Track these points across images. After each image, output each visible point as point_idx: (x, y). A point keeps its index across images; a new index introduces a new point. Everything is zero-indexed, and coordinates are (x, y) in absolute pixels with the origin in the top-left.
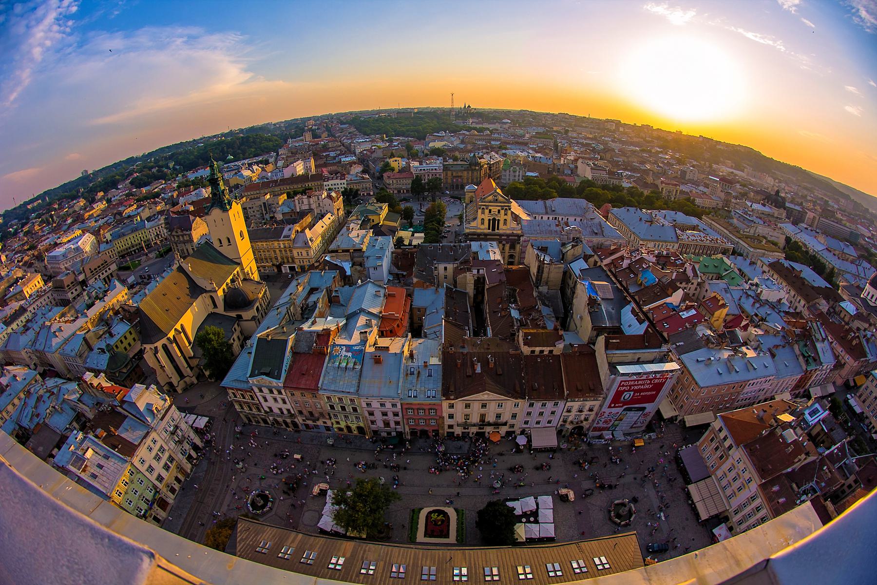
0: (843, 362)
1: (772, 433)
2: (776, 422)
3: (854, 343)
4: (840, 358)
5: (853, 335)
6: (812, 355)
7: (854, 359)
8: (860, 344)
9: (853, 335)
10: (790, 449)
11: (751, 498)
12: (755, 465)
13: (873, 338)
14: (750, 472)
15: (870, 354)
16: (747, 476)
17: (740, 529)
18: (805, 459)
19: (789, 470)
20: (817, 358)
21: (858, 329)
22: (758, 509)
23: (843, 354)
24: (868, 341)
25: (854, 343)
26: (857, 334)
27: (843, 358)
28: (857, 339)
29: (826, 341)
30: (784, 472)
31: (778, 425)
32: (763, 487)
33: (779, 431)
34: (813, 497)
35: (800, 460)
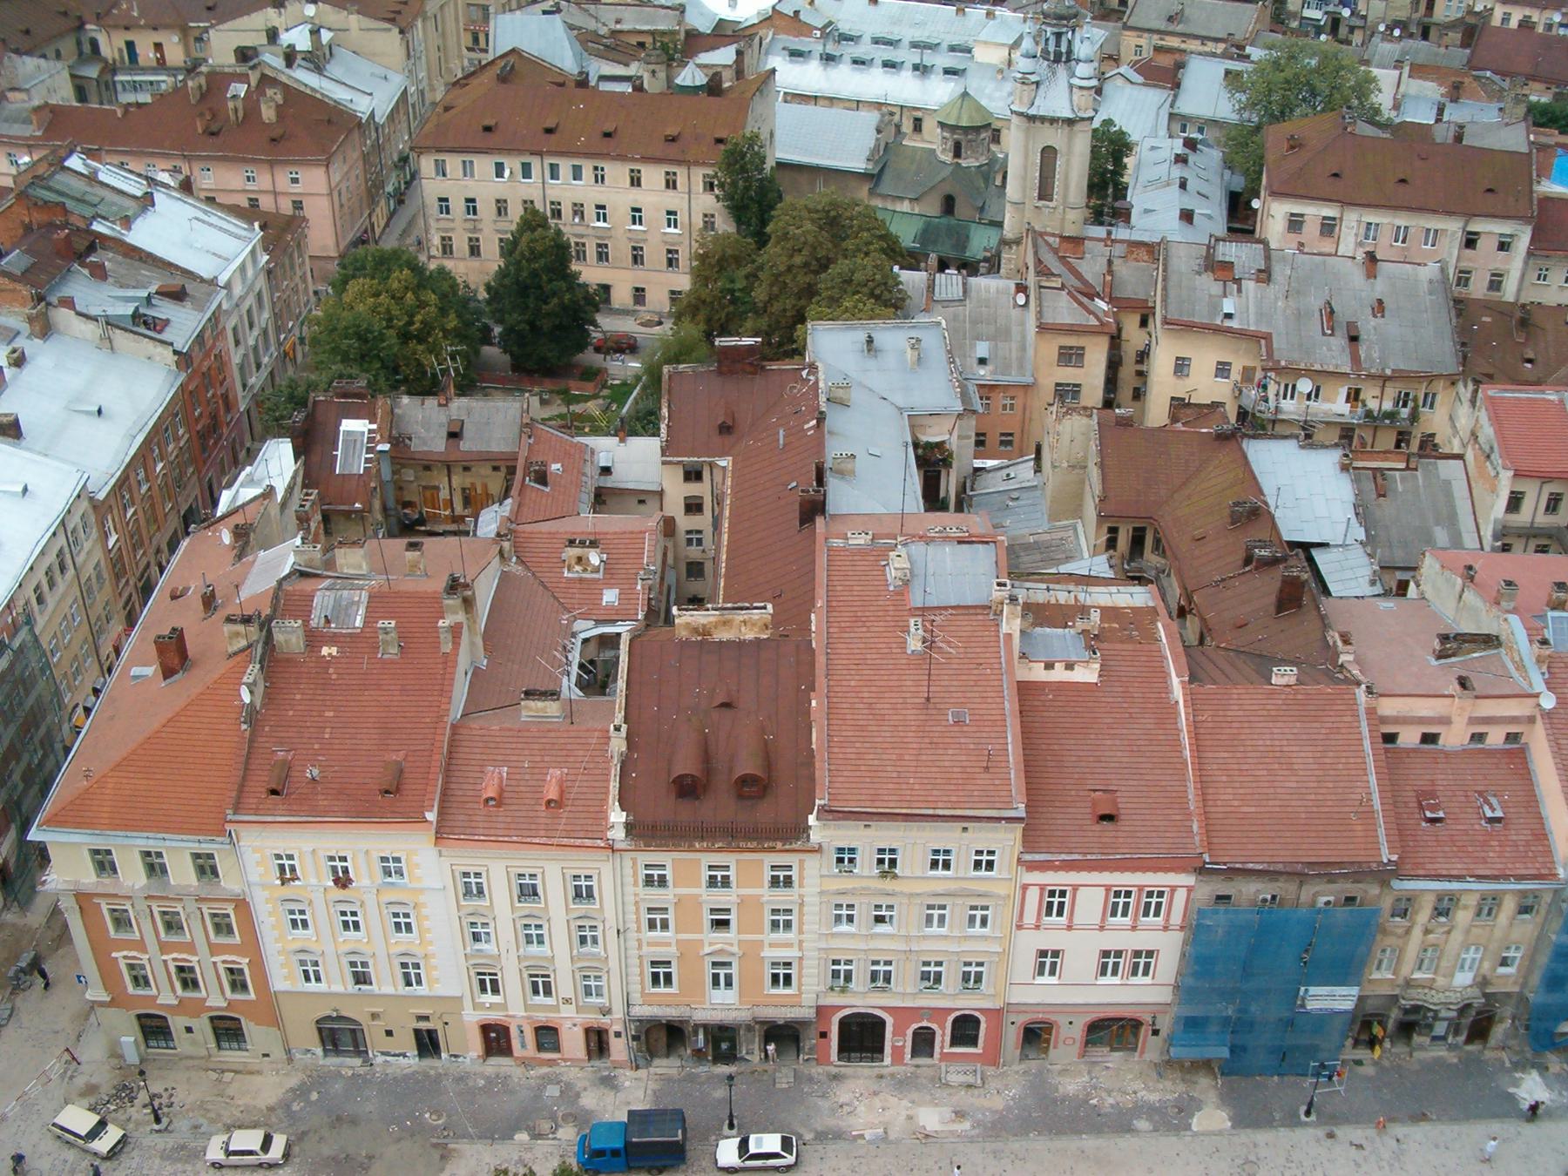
0: (286, 207)
3: (268, 113)
4: (266, 203)
5: (241, 89)
6: (153, 289)
7: (316, 163)
8: (296, 99)
9: (241, 89)
13: (326, 36)
15: (357, 97)
20: (177, 281)
21: (244, 54)
23: (263, 180)
24: (317, 59)
25: (268, 113)
26: (254, 78)
27: (275, 193)
28: (270, 92)
29: (159, 197)
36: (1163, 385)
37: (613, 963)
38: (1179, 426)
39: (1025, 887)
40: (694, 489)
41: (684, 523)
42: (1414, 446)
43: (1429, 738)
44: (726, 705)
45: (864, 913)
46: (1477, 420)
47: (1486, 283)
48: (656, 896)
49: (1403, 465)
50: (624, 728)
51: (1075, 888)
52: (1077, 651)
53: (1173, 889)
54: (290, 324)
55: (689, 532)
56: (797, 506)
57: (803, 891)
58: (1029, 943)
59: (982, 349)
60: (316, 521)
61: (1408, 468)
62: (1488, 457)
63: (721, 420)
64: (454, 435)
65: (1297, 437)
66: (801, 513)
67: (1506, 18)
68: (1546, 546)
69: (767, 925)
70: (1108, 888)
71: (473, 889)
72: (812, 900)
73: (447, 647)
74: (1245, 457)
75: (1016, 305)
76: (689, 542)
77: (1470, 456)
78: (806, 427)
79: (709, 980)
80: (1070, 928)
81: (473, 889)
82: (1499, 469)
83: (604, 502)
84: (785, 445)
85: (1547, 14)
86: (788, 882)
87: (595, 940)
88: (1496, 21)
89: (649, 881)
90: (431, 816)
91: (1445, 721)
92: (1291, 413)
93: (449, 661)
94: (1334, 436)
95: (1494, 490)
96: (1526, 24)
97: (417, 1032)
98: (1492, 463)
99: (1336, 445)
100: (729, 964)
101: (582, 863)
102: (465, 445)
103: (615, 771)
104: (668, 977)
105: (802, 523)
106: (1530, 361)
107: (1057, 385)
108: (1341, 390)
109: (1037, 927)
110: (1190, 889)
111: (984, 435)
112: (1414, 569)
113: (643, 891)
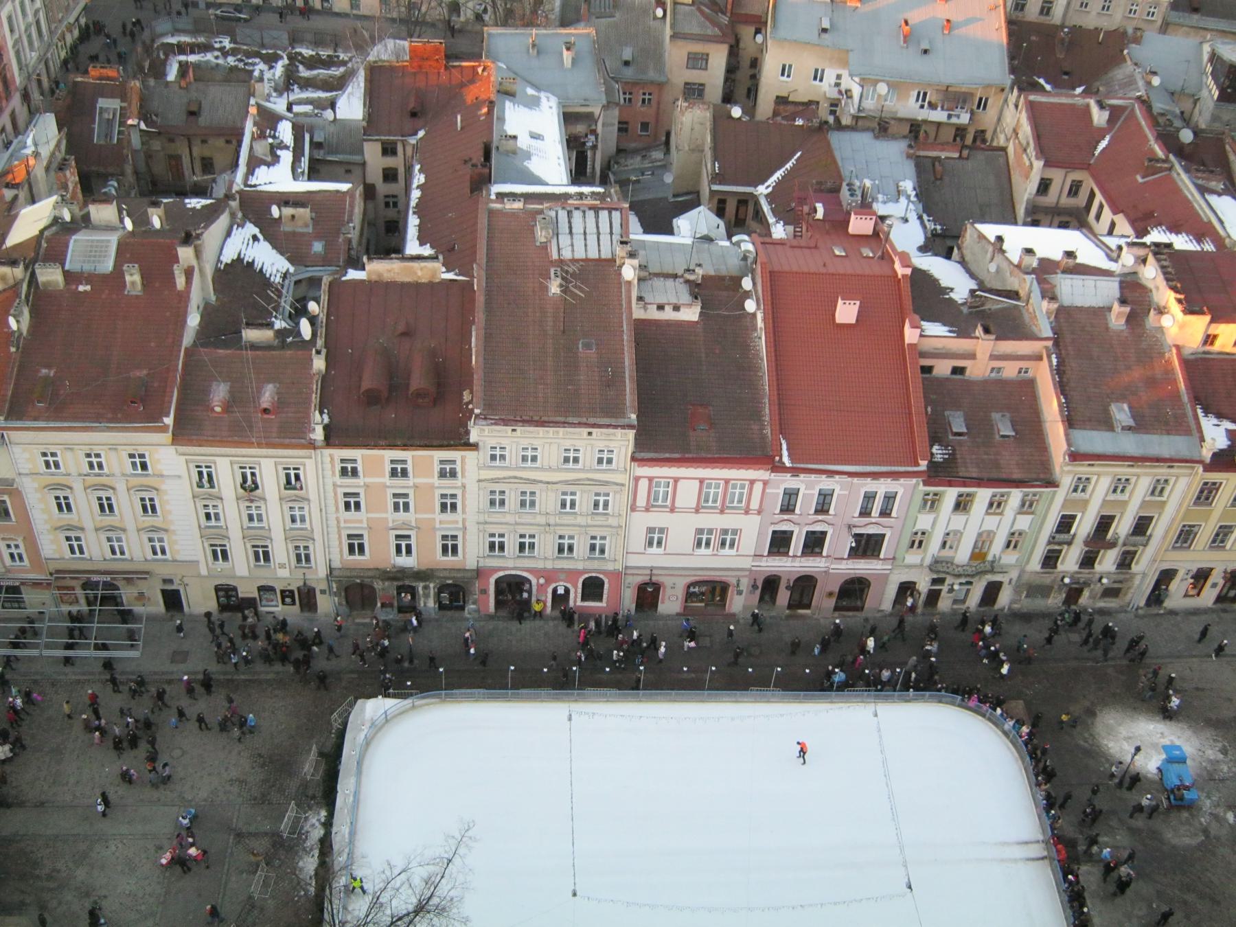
1: (40, 299)
2: (13, 263)
10: (133, 278)
11: (200, 485)
12: (98, 418)
14: (113, 447)
16: (117, 463)
17: (282, 566)
18: (198, 254)
19: (194, 320)
22: (249, 486)
30: (188, 339)
31: (29, 265)
32: (184, 433)
33: (50, 275)
34: (324, 298)
35: (189, 273)
36: (771, 82)
37: (317, 535)
38: (779, 119)
39: (637, 479)
40: (390, 162)
41: (382, 188)
42: (969, 140)
43: (958, 371)
44: (405, 334)
45: (512, 500)
46: (1018, 121)
47: (1038, 9)
48: (350, 484)
49: (956, 155)
50: (324, 351)
51: (676, 480)
52: (685, 297)
53: (752, 482)
54: (60, 15)
55: (386, 196)
56: (468, 177)
57: (464, 481)
58: (641, 522)
59: (627, 54)
60: (72, 177)
61: (960, 157)
62: (1025, 150)
63: (411, 105)
64: (193, 114)
65: (873, 130)
66: (471, 182)
68: (1067, 222)
69: (438, 507)
70: (702, 481)
71: (205, 479)
72: (472, 487)
73: (180, 282)
74: (828, 144)
75: (655, 18)
76: (387, 205)
77: (1011, 150)
78: (479, 113)
79: (393, 550)
80: (672, 510)
81: (205, 479)
82: (1033, 159)
83: (318, 171)
84: (462, 128)
86: (453, 474)
87: (303, 520)
89: (344, 472)
90: (169, 421)
91: (972, 356)
92: (870, 110)
93: (184, 297)
94: (906, 129)
95: (1027, 177)
97: (164, 592)
98: (1027, 155)
99: (905, 137)
100: (409, 537)
101: (292, 457)
102: (203, 121)
103: (315, 387)
104: (361, 547)
105: (472, 191)
106: (1066, 73)
107: (686, 84)
108: (912, 93)
109: (647, 510)
110: (765, 483)
111: (626, 123)
112: (958, 237)
113: (339, 480)
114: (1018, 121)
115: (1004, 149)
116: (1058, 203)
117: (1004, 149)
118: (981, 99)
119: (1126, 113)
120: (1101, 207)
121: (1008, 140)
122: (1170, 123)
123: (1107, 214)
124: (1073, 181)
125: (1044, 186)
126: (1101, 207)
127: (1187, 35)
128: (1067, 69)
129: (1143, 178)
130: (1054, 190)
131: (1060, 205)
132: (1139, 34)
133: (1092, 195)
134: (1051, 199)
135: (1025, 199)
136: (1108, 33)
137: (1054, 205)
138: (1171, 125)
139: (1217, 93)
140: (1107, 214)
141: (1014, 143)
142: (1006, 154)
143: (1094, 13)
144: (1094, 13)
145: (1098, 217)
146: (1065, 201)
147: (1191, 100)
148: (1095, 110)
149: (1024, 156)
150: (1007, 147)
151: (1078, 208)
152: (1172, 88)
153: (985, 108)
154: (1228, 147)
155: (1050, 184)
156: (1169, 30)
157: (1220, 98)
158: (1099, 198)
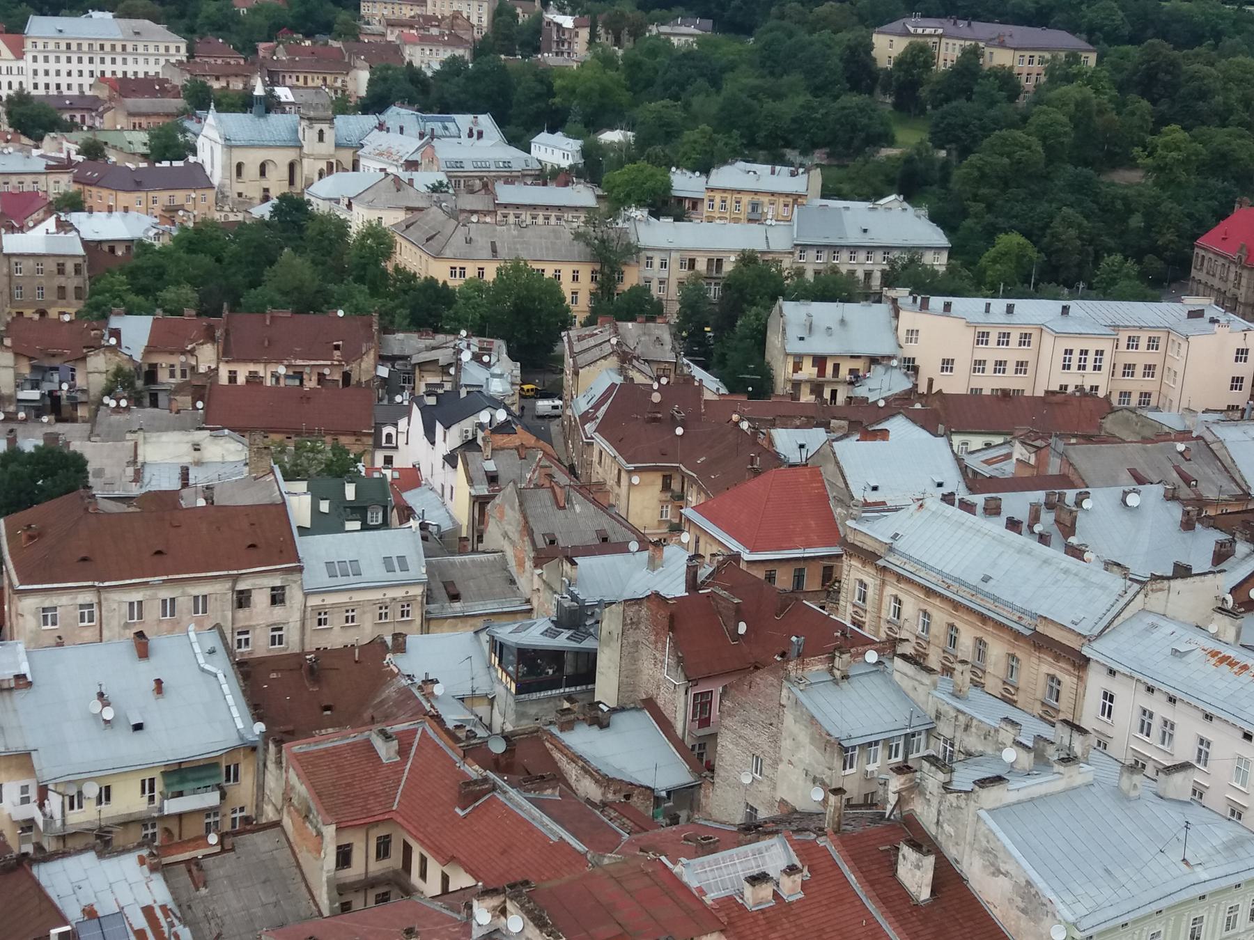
67: (233, 377)
85: (272, 368)
88: (224, 379)
96: (253, 378)
114: (287, 781)
115: (277, 824)
116: (366, 873)
117: (277, 824)
118: (228, 768)
119: (418, 736)
120: (423, 860)
121: (279, 811)
122: (471, 735)
123: (435, 870)
124: (379, 838)
125: (344, 856)
126: (423, 860)
127: (454, 628)
128: (326, 703)
129: (464, 809)
130: (357, 857)
131: (370, 875)
132: (401, 639)
133: (407, 849)
134: (356, 871)
135: (324, 879)
136: (362, 647)
137: (363, 877)
138: (475, 737)
139: (513, 685)
140: (434, 870)
141: (289, 812)
142: (282, 827)
143: (337, 628)
144: (337, 628)
145: (423, 875)
146: (376, 867)
147: (486, 701)
148: (378, 743)
149: (308, 824)
150: (281, 821)
151: (395, 872)
152: (460, 694)
153: (236, 779)
154: (547, 744)
155: (351, 851)
156: (432, 628)
157: (519, 691)
158: (417, 850)
